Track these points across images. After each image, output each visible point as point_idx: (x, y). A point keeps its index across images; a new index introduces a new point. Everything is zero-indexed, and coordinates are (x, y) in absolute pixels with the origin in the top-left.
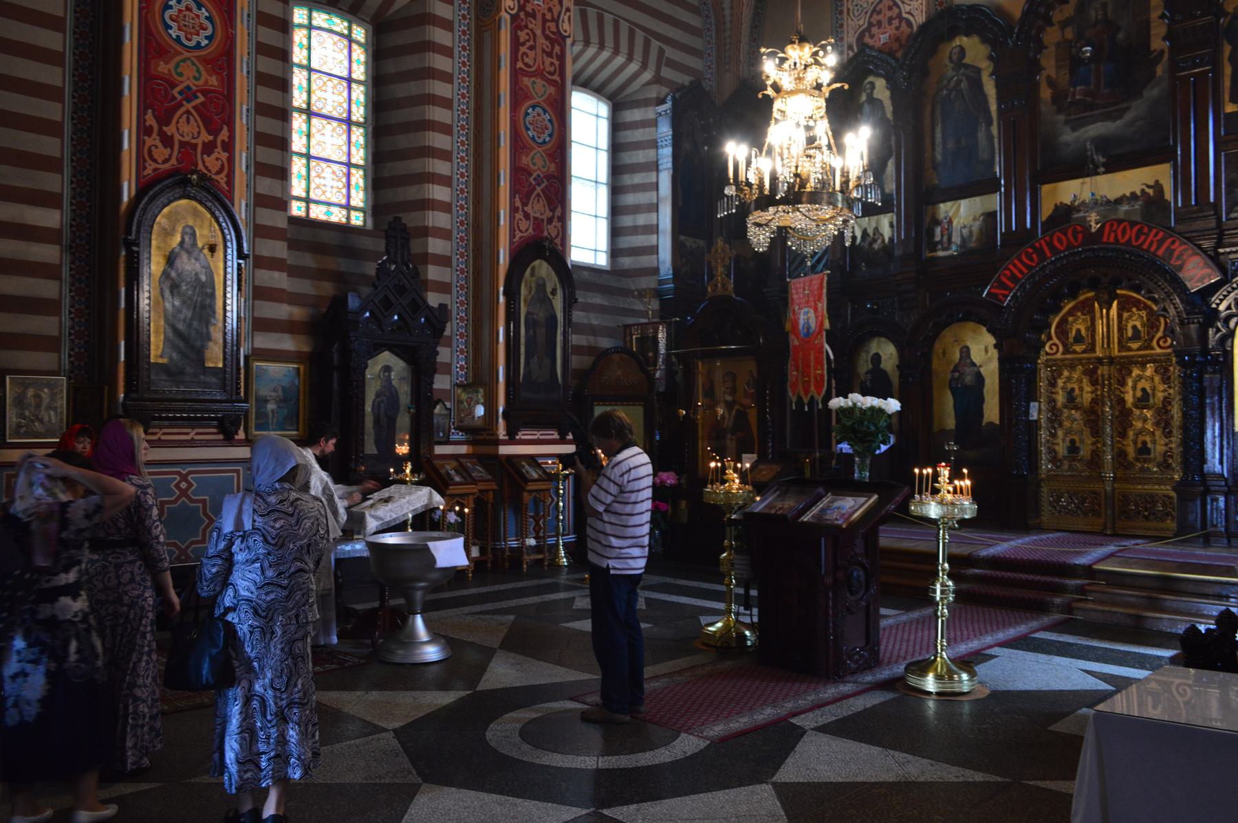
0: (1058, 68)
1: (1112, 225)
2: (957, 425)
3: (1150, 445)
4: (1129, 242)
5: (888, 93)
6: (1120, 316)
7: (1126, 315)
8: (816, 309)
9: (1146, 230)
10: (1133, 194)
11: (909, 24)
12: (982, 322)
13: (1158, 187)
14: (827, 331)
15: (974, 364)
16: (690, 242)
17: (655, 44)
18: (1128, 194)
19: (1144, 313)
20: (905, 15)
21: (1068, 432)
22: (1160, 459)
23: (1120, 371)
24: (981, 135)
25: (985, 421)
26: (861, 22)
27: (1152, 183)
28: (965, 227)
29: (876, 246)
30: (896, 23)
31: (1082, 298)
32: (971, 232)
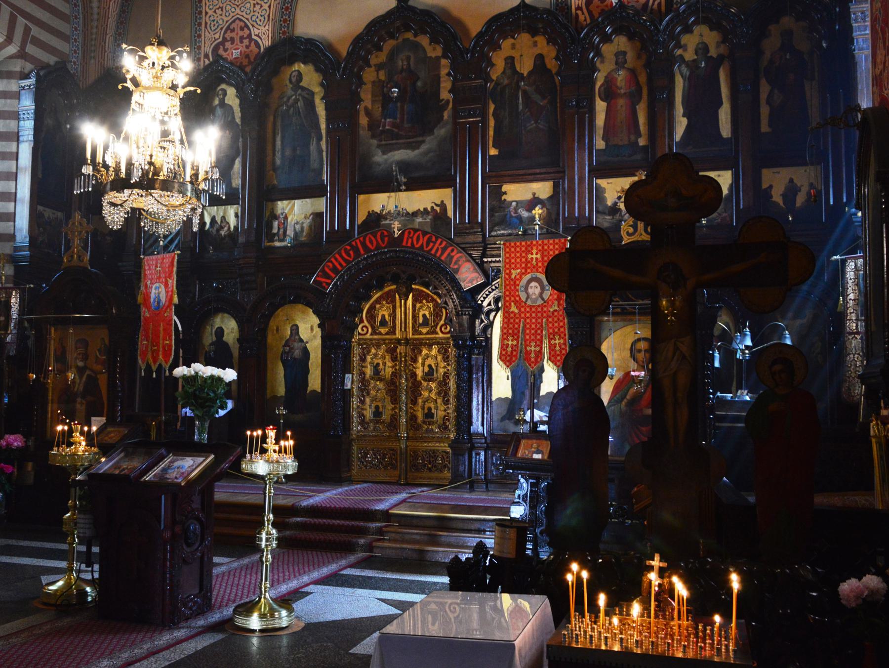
0: (373, 102)
1: (409, 233)
2: (286, 392)
3: (433, 411)
5: (237, 101)
6: (414, 306)
7: (418, 305)
8: (166, 285)
9: (434, 239)
10: (425, 209)
11: (257, 45)
12: (309, 305)
13: (443, 205)
14: (176, 305)
15: (301, 340)
16: (48, 213)
17: (21, 21)
18: (422, 209)
19: (431, 305)
20: (254, 37)
21: (374, 399)
22: (440, 422)
23: (413, 350)
24: (313, 147)
26: (217, 36)
27: (439, 202)
28: (297, 223)
29: (223, 233)
30: (246, 42)
31: (386, 289)
32: (302, 228)
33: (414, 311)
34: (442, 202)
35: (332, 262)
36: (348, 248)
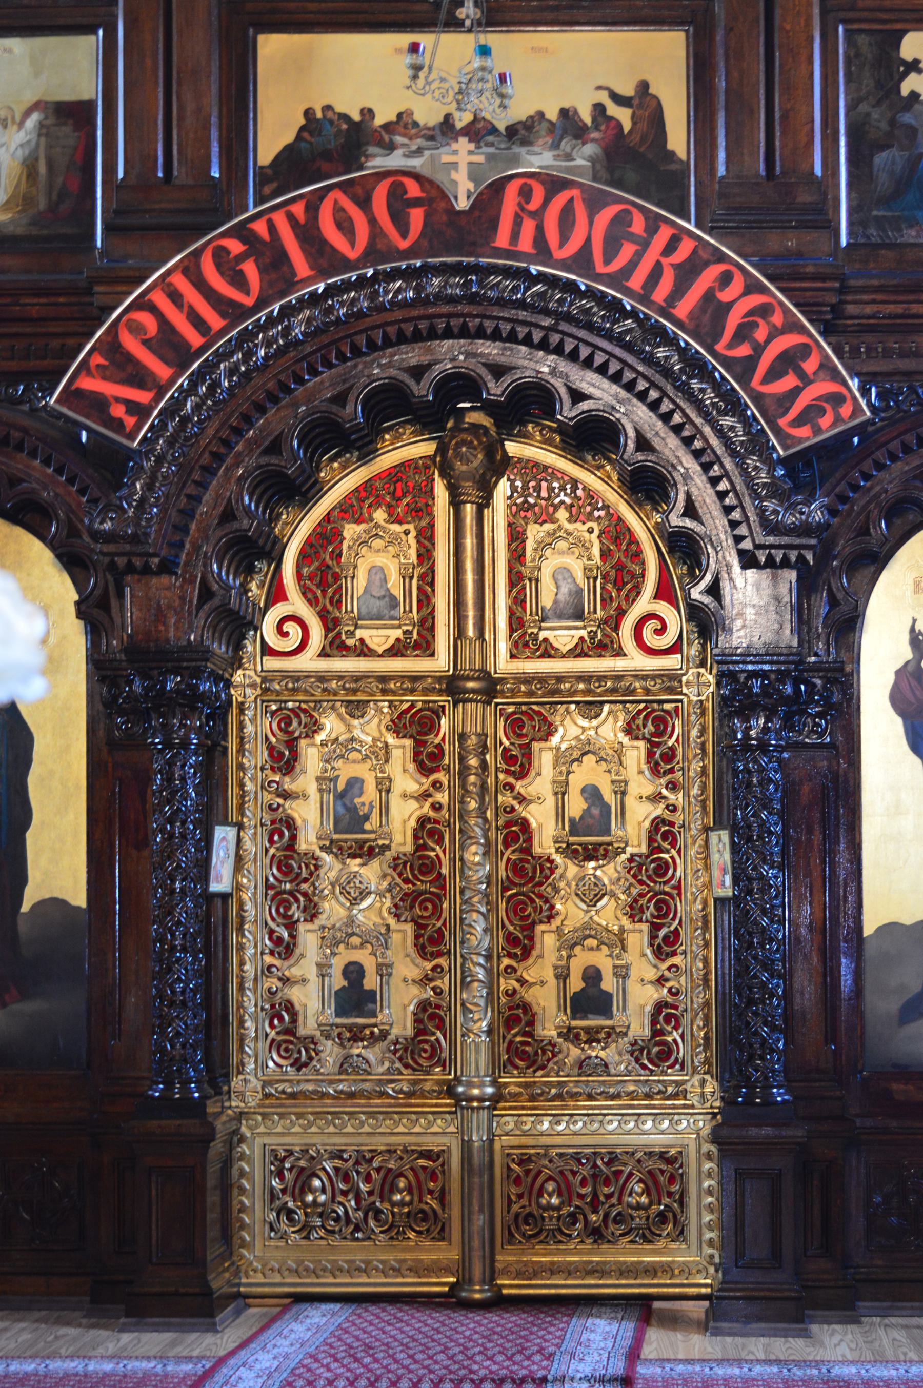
3: (608, 984)
4: (582, 261)
6: (516, 537)
13: (644, 101)
18: (552, 115)
21: (334, 940)
22: (640, 1029)
23: (515, 725)
25: (31, 897)
27: (627, 90)
31: (388, 459)
33: (517, 555)
34: (644, 87)
35: (153, 309)
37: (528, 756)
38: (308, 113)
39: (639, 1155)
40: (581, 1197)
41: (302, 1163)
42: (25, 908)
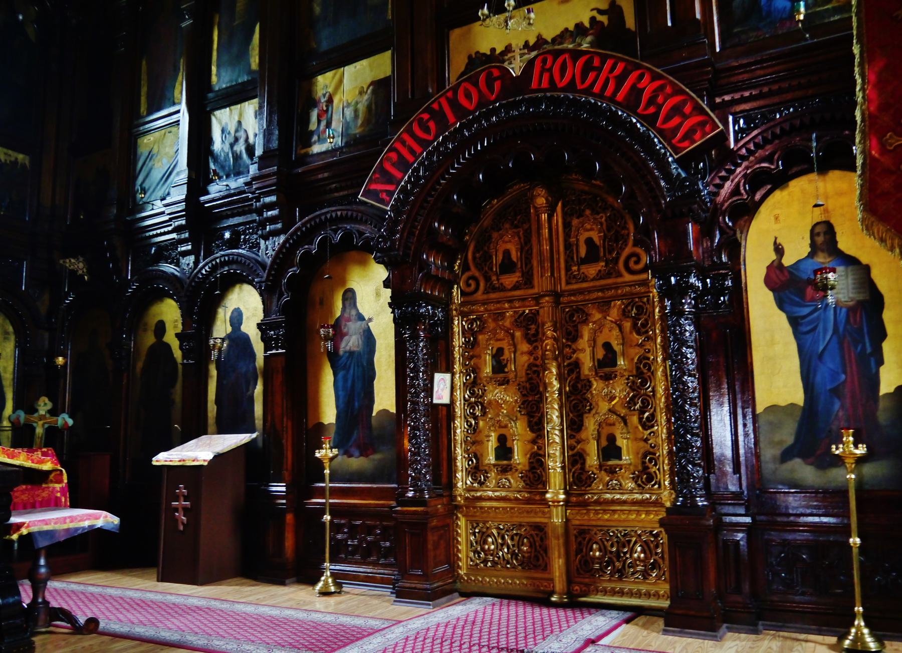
1: (544, 61)
6: (567, 225)
15: (361, 318)
18: (571, 27)
25: (377, 408)
27: (604, 6)
28: (349, 105)
32: (356, 111)
33: (567, 235)
36: (426, 116)
37: (577, 331)
38: (470, 57)
39: (639, 532)
40: (611, 552)
41: (484, 530)
42: (374, 414)
